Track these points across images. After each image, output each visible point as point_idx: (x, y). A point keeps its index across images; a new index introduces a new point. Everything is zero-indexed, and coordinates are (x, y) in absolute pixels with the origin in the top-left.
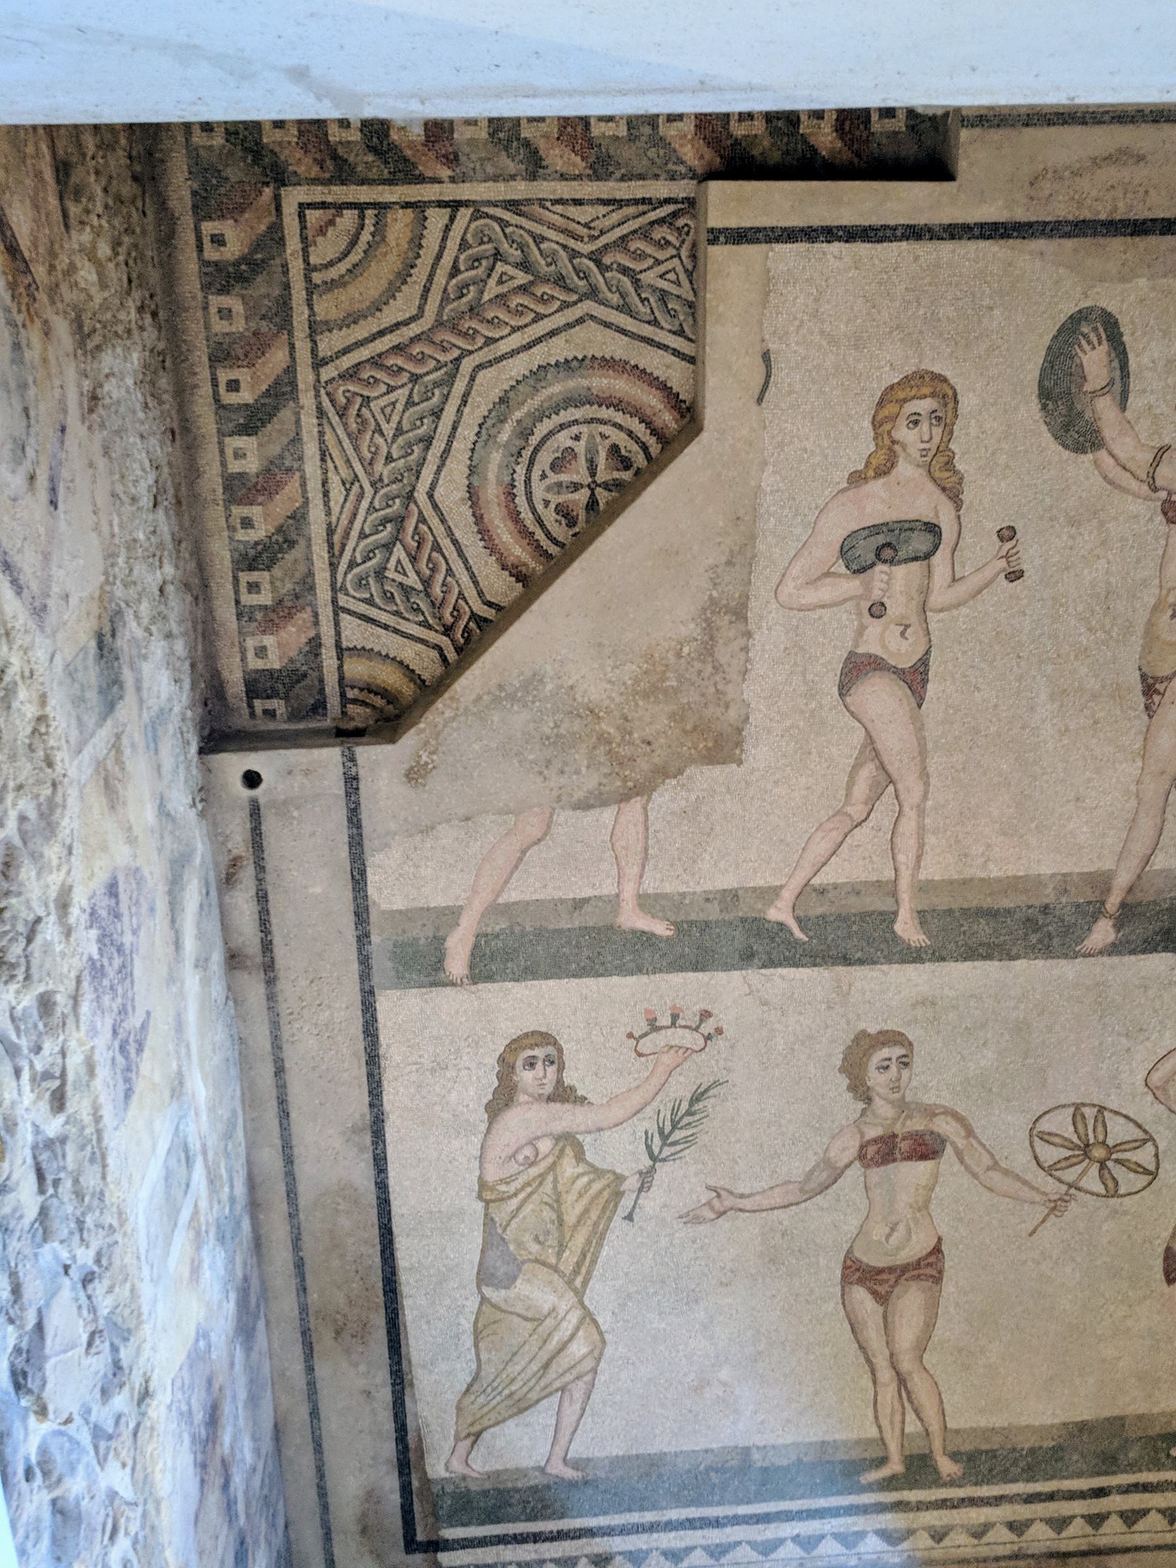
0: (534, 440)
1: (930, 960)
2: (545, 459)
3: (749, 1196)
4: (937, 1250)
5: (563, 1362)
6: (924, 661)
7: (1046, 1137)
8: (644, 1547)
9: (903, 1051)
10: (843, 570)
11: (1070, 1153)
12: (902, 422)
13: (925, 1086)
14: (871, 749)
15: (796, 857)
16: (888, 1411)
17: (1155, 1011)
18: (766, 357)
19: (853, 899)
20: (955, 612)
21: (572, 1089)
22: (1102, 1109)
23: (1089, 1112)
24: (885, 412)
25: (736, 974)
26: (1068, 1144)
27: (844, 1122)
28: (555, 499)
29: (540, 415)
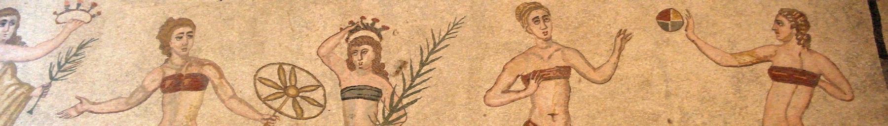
7: (263, 81)
9: (188, 29)
11: (276, 91)
13: (200, 49)
17: (321, 15)
21: (20, 38)
22: (294, 67)
26: (274, 85)
27: (155, 66)
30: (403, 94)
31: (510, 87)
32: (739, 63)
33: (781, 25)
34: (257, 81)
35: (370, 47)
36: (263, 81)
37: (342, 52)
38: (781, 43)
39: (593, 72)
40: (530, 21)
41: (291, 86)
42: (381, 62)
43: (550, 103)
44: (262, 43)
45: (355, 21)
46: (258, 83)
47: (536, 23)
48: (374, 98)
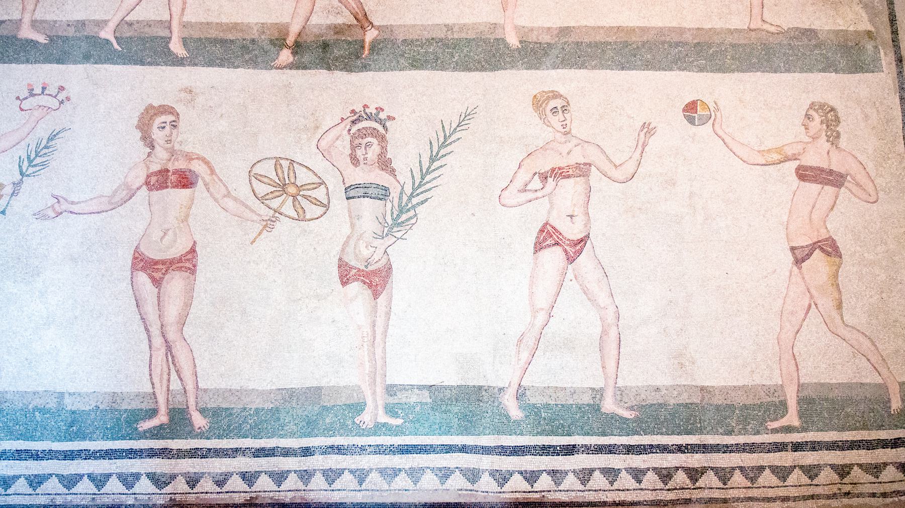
1: (189, 65)
4: (193, 251)
7: (259, 178)
9: (173, 118)
11: (275, 189)
16: (158, 371)
19: (147, 29)
23: (285, 164)
25: (80, 67)
27: (137, 160)
30: (412, 193)
32: (767, 161)
33: (811, 119)
34: (253, 178)
35: (375, 139)
36: (259, 177)
37: (344, 147)
38: (811, 140)
39: (614, 169)
42: (387, 157)
45: (357, 111)
47: (555, 114)
48: (381, 197)
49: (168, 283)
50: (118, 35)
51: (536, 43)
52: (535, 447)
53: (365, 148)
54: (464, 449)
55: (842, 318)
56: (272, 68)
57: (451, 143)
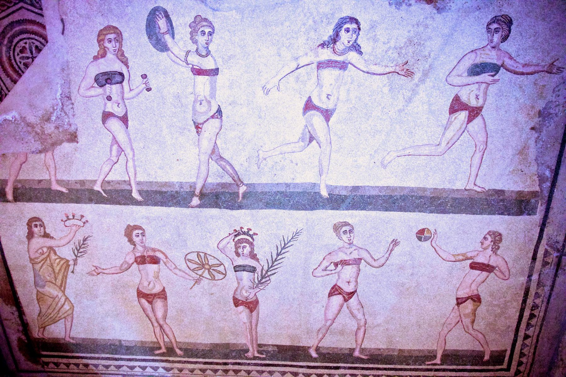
0: (14, 44)
2: (17, 50)
3: (106, 269)
4: (164, 290)
5: (63, 310)
6: (126, 114)
7: (190, 261)
8: (97, 363)
9: (142, 232)
10: (96, 86)
12: (106, 41)
14: (115, 140)
15: (99, 171)
16: (159, 334)
18: (62, 20)
19: (118, 185)
20: (132, 100)
22: (206, 254)
24: (101, 38)
26: (196, 263)
28: (23, 62)
29: (14, 36)
30: (268, 270)
31: (327, 268)
40: (341, 233)
41: (206, 264)
43: (348, 276)
44: (185, 241)
45: (237, 230)
46: (187, 262)
49: (155, 303)
50: (103, 188)
51: (338, 195)
52: (322, 367)
53: (243, 248)
54: (291, 366)
55: (473, 327)
56: (189, 207)
57: (288, 247)
